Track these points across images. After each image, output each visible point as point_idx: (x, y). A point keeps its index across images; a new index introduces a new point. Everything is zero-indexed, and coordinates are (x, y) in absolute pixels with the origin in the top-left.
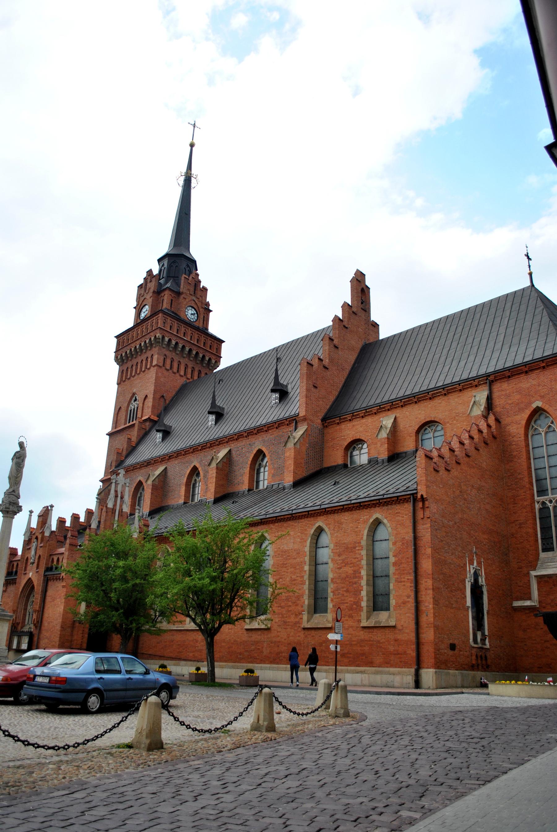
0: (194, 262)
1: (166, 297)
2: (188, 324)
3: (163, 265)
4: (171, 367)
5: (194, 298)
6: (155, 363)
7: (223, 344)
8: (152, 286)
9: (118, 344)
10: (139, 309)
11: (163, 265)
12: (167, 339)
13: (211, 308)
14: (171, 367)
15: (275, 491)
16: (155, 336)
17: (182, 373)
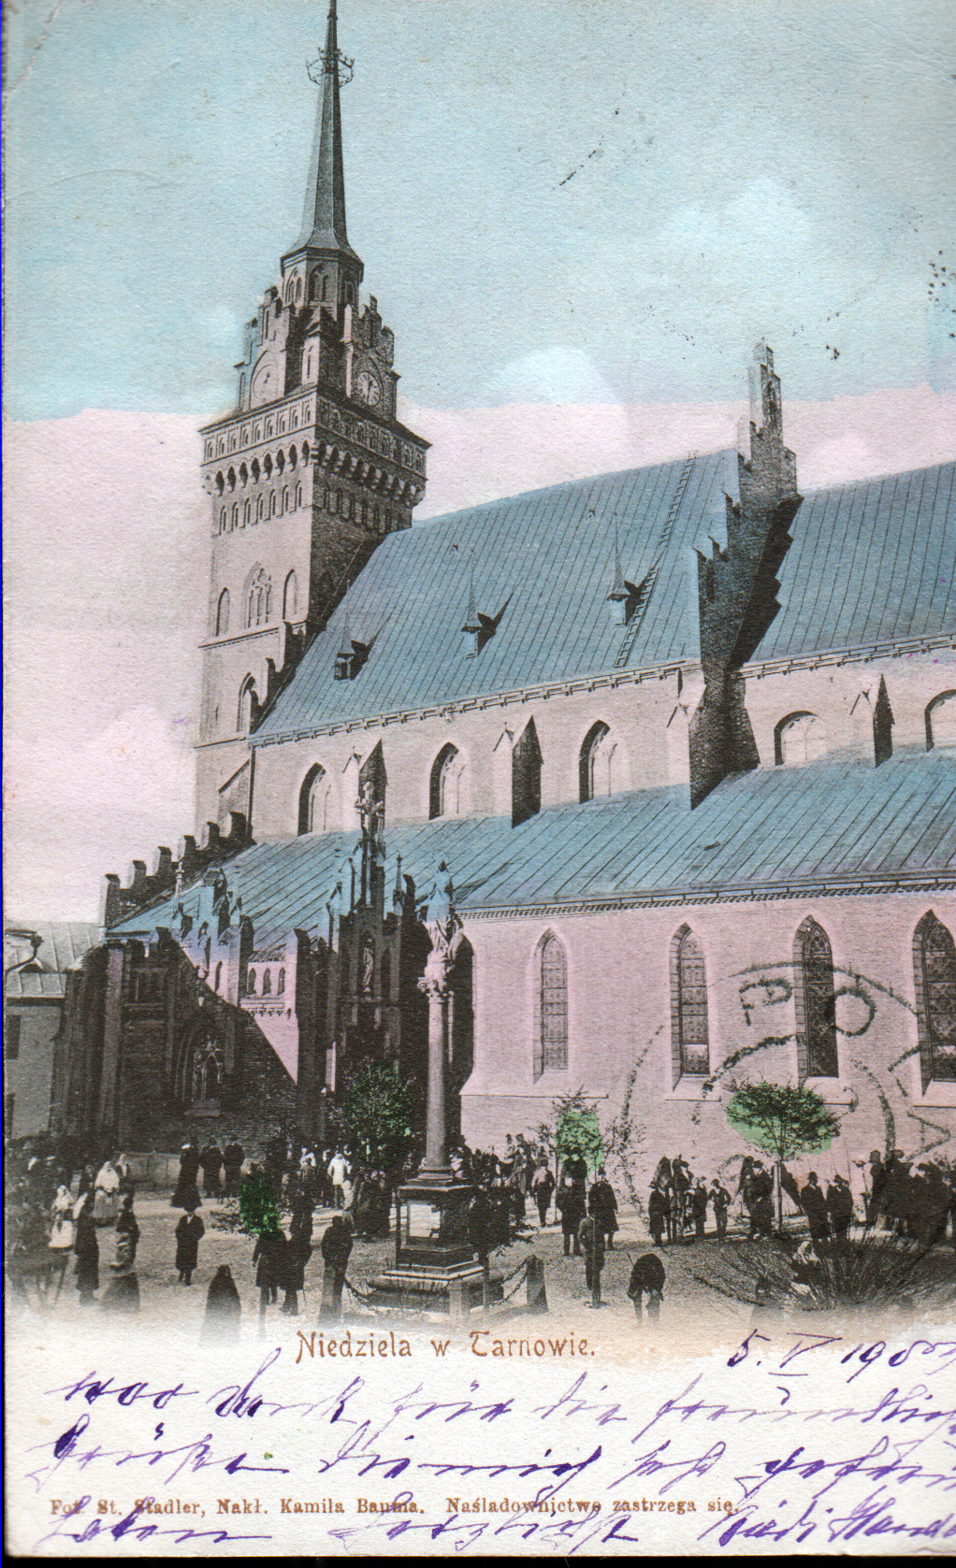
0: (360, 266)
1: (313, 346)
2: (366, 413)
3: (295, 272)
4: (339, 507)
5: (374, 356)
6: (308, 498)
7: (429, 452)
8: (281, 327)
9: (208, 450)
10: (247, 370)
11: (295, 272)
12: (329, 449)
13: (396, 368)
14: (339, 507)
15: (644, 802)
16: (306, 445)
17: (358, 520)
